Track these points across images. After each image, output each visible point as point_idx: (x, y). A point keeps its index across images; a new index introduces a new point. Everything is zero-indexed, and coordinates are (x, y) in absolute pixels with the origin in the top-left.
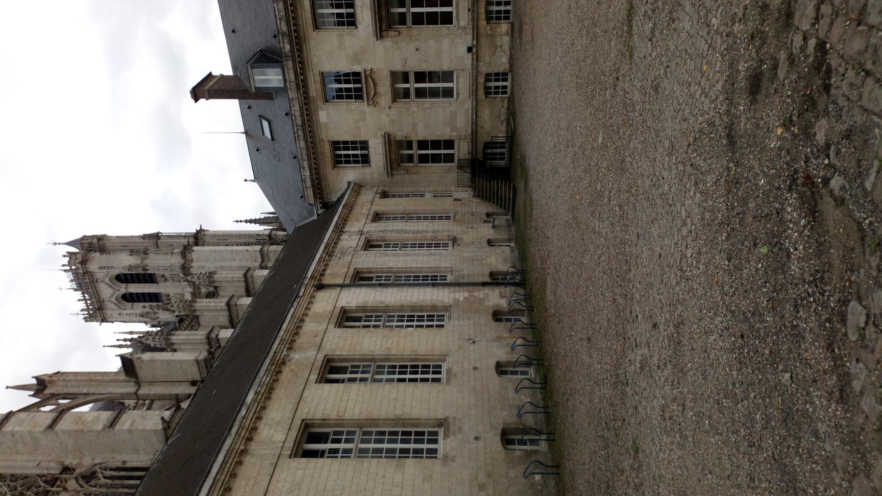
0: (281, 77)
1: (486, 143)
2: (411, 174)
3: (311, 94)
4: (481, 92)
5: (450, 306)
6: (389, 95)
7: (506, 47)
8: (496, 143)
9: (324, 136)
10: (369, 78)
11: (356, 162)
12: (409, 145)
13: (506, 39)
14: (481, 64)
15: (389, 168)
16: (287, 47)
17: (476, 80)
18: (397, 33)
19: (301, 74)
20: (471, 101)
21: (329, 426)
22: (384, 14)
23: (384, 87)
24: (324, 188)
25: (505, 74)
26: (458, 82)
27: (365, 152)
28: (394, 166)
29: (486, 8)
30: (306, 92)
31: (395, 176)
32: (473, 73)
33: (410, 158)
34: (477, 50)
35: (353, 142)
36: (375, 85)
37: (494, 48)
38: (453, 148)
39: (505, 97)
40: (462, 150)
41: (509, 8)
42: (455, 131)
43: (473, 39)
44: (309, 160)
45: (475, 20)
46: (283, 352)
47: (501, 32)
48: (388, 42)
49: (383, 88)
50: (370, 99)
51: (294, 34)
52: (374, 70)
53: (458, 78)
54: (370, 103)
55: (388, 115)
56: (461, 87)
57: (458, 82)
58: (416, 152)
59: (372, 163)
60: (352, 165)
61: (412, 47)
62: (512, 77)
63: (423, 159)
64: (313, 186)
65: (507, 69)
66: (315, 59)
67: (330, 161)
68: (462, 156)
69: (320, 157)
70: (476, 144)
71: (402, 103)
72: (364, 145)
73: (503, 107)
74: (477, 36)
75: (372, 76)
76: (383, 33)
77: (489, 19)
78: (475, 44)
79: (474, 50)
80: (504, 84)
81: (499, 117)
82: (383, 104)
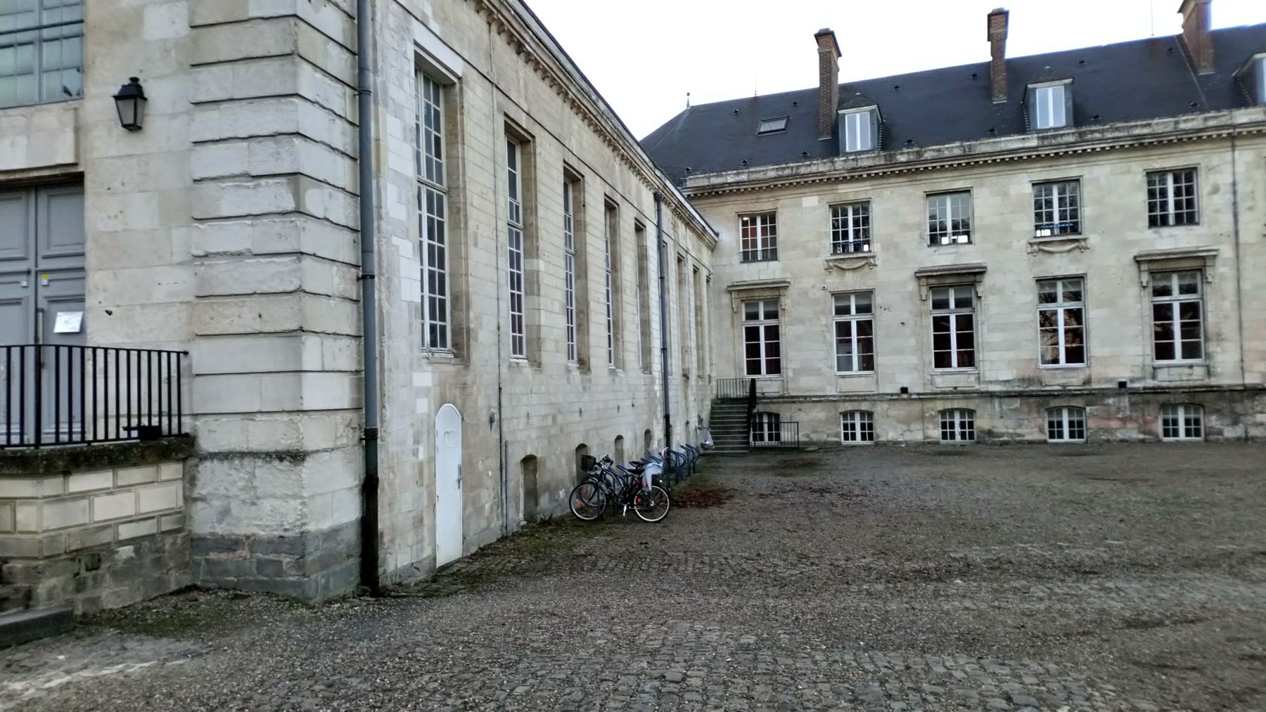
0: (859, 148)
1: (777, 416)
3: (840, 187)
4: (848, 407)
5: (651, 373)
6: (841, 288)
8: (778, 428)
9: (781, 202)
10: (864, 263)
11: (745, 244)
12: (771, 315)
13: (919, 436)
14: (885, 406)
16: (903, 158)
17: (865, 400)
19: (868, 175)
21: (575, 212)
22: (949, 281)
23: (851, 282)
24: (709, 201)
25: (871, 437)
26: (860, 376)
28: (744, 295)
29: (957, 409)
30: (845, 180)
31: (729, 296)
32: (874, 395)
33: (752, 316)
34: (904, 399)
35: (774, 241)
36: (854, 269)
37: (907, 421)
38: (768, 372)
39: (840, 437)
40: (768, 385)
41: (958, 438)
42: (794, 374)
43: (918, 394)
44: (749, 182)
47: (928, 429)
48: (912, 286)
51: (921, 167)
52: (875, 268)
53: (866, 376)
57: (860, 376)
59: (746, 265)
60: (741, 239)
61: (906, 316)
62: (869, 446)
63: (752, 334)
64: (714, 186)
68: (758, 384)
69: (754, 197)
70: (778, 403)
71: (832, 304)
72: (771, 255)
74: (922, 398)
78: (913, 397)
79: (905, 396)
80: (858, 436)
81: (814, 432)
82: (829, 281)
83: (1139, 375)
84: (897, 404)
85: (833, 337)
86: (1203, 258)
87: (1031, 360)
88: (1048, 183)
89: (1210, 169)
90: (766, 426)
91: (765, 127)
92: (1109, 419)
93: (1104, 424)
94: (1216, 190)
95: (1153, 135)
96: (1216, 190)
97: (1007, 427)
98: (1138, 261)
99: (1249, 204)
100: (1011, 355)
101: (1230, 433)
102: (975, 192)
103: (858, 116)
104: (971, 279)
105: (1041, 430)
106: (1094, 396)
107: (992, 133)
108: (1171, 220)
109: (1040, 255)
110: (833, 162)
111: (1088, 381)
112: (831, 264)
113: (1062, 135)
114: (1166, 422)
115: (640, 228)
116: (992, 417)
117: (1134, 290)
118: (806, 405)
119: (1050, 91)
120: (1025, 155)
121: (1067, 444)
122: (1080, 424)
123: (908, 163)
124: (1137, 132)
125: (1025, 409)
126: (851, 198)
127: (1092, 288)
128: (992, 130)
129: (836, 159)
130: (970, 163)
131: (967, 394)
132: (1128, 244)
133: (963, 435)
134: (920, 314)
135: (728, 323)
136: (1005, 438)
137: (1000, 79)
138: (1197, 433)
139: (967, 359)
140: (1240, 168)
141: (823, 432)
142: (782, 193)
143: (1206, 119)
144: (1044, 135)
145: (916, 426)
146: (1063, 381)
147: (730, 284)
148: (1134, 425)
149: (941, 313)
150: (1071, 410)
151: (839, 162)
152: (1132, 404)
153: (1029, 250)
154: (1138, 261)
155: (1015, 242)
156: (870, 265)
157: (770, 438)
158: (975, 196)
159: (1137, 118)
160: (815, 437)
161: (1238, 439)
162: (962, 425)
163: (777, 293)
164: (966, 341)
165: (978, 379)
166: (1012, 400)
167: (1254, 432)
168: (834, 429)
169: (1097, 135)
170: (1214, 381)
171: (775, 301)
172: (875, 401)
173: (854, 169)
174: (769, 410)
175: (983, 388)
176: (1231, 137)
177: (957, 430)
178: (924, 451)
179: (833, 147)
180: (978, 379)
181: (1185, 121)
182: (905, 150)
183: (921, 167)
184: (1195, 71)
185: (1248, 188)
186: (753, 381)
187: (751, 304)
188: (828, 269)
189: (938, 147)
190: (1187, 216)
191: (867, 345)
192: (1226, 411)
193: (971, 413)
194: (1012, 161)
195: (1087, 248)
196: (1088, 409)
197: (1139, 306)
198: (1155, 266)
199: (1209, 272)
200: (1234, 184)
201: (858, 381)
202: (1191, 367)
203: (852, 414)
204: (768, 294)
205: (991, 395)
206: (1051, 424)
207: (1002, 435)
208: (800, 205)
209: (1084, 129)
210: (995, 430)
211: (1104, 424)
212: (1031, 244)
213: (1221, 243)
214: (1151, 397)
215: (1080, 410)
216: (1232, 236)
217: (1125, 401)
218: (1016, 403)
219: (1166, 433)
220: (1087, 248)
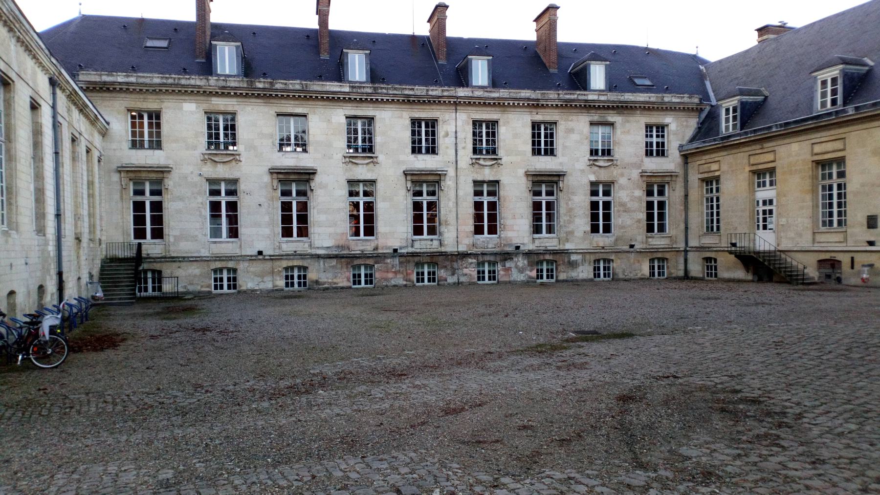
0: (227, 72)
1: (160, 272)
2: (121, 193)
4: (218, 265)
5: (44, 235)
6: (214, 176)
7: (262, 286)
8: (160, 282)
10: (231, 158)
11: (134, 134)
13: (269, 286)
14: (246, 264)
15: (128, 169)
16: (260, 85)
17: (231, 260)
18: (275, 188)
19: (235, 93)
20: (208, 255)
22: (292, 177)
23: (222, 171)
24: (100, 95)
25: (235, 287)
26: (228, 242)
27: (146, 145)
28: (132, 175)
30: (216, 94)
31: (118, 175)
32: (238, 256)
33: (141, 193)
34: (260, 259)
35: (159, 134)
37: (262, 275)
38: (153, 237)
40: (151, 247)
41: (296, 286)
42: (175, 240)
43: (270, 256)
44: (138, 84)
45: (288, 256)
46: (19, 31)
48: (267, 178)
49: (221, 170)
50: (210, 157)
51: (274, 94)
52: (240, 163)
53: (232, 242)
54: (206, 157)
55: (192, 173)
56: (223, 245)
57: (228, 242)
58: (148, 199)
59: (134, 151)
61: (262, 200)
63: (139, 207)
64: (105, 83)
65: (242, 288)
66: (250, 109)
67: (136, 106)
68: (144, 247)
69: (141, 96)
71: (207, 188)
72: (157, 144)
73: (202, 287)
74: (273, 258)
75: (234, 161)
76: (275, 175)
77: (286, 269)
78: (266, 258)
79: (261, 257)
80: (225, 286)
82: (204, 169)
83: (405, 245)
84: (255, 263)
85: (207, 213)
86: (440, 175)
87: (343, 234)
88: (356, 117)
89: (444, 122)
90: (150, 281)
91: (150, 43)
92: (387, 272)
93: (385, 275)
94: (447, 135)
95: (415, 96)
96: (447, 135)
97: (327, 278)
98: (406, 174)
99: (464, 145)
100: (331, 230)
101: (451, 280)
102: (310, 117)
103: (227, 48)
104: (307, 177)
105: (348, 280)
106: (378, 257)
107: (320, 78)
108: (424, 151)
109: (350, 164)
110: (208, 80)
111: (376, 248)
112: (206, 157)
113: (364, 87)
114: (418, 274)
115: (35, 107)
116: (318, 271)
117: (403, 192)
118: (184, 264)
119: (357, 56)
120: (342, 97)
121: (363, 288)
122: (371, 275)
123: (264, 89)
124: (407, 92)
125: (339, 266)
126: (222, 108)
127: (381, 189)
128: (320, 76)
129: (210, 78)
130: (307, 97)
131: (303, 256)
132: (400, 163)
133: (299, 284)
134: (272, 199)
135: (117, 196)
136: (326, 286)
137: (325, 41)
138: (434, 281)
139: (303, 232)
140: (459, 123)
141: (198, 284)
142: (166, 97)
143: (443, 91)
144: (354, 85)
145: (268, 279)
146: (362, 248)
147: (120, 165)
148: (401, 276)
149: (286, 199)
150: (367, 266)
151: (213, 80)
152: (400, 263)
153: (344, 161)
154: (406, 174)
155: (335, 155)
156: (237, 160)
157: (154, 289)
158: (310, 120)
159: (407, 84)
160: (191, 288)
161: (454, 284)
162: (299, 277)
163: (160, 175)
164: (303, 219)
165: (311, 246)
166: (331, 260)
167: (462, 279)
168: (207, 281)
169: (384, 91)
170: (443, 249)
171: (160, 182)
172: (239, 260)
173: (224, 88)
174: (152, 267)
175: (314, 252)
176: (455, 104)
177: (296, 280)
178: (273, 295)
179: (208, 68)
180: (311, 246)
181: (432, 90)
182: (262, 80)
183: (274, 94)
184: (437, 62)
185: (463, 136)
186: (140, 245)
187: (138, 182)
188: (204, 160)
189: (285, 81)
190: (432, 150)
191: (233, 220)
192: (449, 267)
193: (305, 268)
194: (333, 99)
195: (377, 163)
196: (376, 266)
197: (405, 202)
198: (415, 178)
199: (442, 183)
200: (456, 132)
201: (226, 246)
202: (432, 240)
203: (221, 270)
204: (154, 176)
205: (318, 257)
206: (354, 276)
207: (324, 283)
208: (181, 108)
209: (377, 85)
210: (320, 280)
211: (385, 275)
212: (345, 157)
213: (448, 167)
214: (411, 258)
215: (372, 267)
216: (454, 163)
217: (397, 261)
218: (334, 262)
219: (418, 281)
220: (377, 163)
